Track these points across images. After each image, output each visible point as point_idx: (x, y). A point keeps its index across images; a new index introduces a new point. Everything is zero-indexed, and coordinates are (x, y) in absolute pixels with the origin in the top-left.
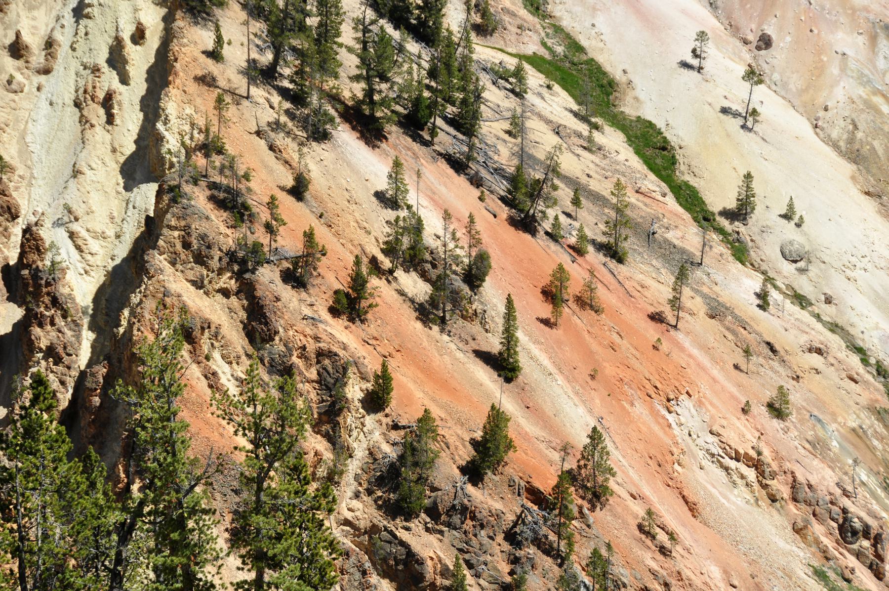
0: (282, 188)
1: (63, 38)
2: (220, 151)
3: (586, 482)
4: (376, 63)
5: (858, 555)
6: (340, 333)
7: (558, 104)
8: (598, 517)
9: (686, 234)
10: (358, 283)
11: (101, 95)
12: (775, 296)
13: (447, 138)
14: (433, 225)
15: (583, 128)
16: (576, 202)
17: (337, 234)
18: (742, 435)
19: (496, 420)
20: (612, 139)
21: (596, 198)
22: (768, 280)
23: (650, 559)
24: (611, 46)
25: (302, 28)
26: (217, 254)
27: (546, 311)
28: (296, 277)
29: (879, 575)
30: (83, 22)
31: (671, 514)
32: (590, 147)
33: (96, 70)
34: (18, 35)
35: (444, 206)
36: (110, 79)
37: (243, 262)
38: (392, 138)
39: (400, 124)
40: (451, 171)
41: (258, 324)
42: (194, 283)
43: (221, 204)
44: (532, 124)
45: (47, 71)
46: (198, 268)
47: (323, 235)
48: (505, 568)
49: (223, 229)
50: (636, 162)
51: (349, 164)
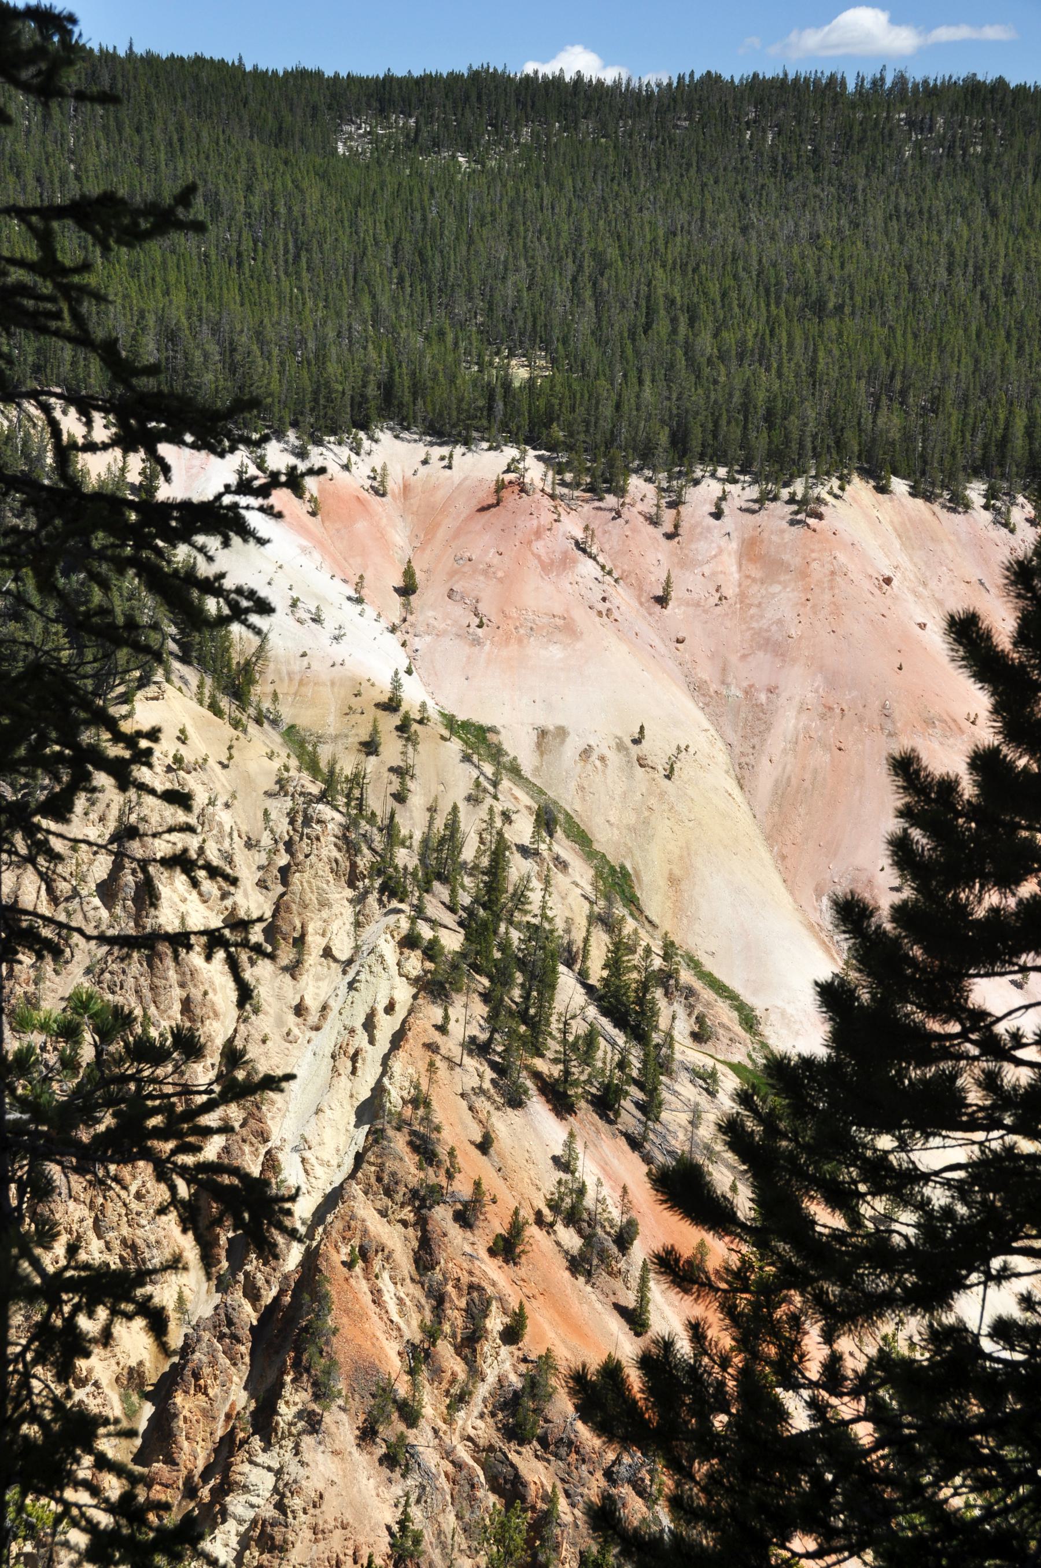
0: (472, 1143)
1: (335, 1005)
11: (351, 1051)
17: (511, 1187)
26: (402, 1190)
30: (353, 993)
33: (352, 1031)
34: (302, 998)
36: (361, 1039)
37: (423, 1200)
38: (580, 1114)
39: (591, 1103)
40: (626, 1148)
42: (380, 1212)
46: (385, 1199)
49: (413, 1170)
51: (535, 1129)
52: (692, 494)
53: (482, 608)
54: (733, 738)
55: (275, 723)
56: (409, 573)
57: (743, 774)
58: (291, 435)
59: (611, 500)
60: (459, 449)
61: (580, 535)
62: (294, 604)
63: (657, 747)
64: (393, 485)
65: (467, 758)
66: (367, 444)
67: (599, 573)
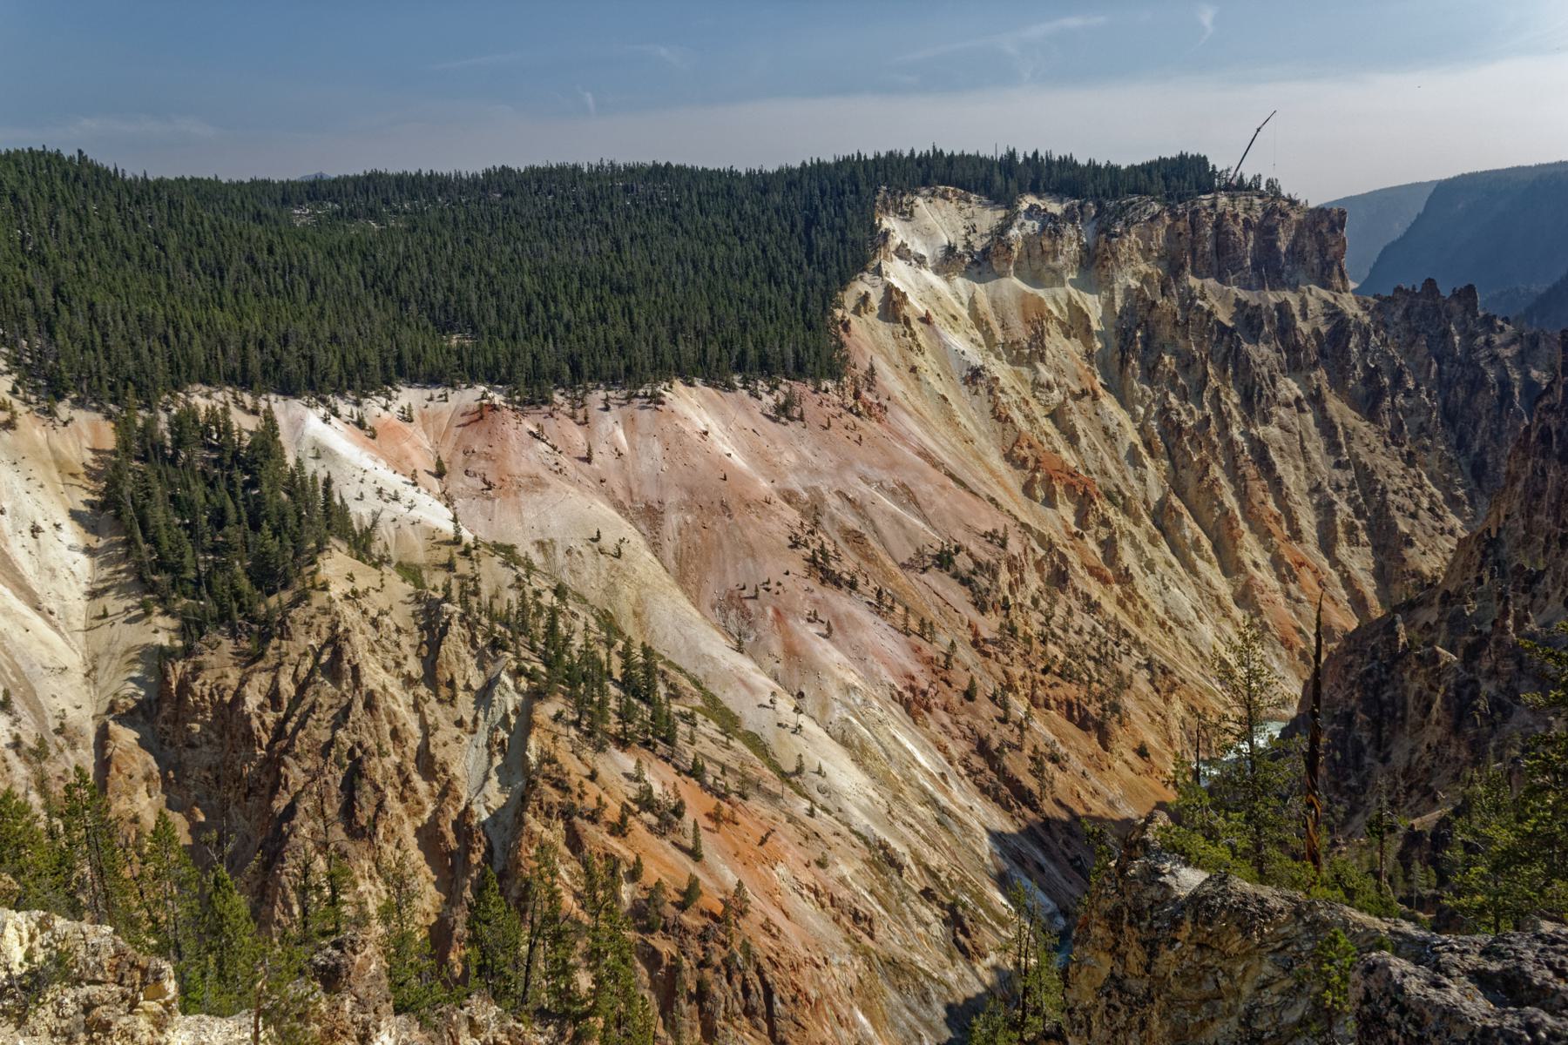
2: (555, 762)
3: (736, 905)
4: (625, 715)
5: (863, 930)
6: (614, 844)
7: (709, 728)
8: (742, 922)
9: (774, 785)
10: (623, 819)
12: (818, 810)
13: (662, 748)
14: (657, 789)
15: (724, 739)
16: (723, 772)
18: (806, 877)
19: (694, 883)
20: (736, 743)
21: (733, 771)
22: (813, 802)
23: (768, 941)
24: (732, 699)
25: (592, 702)
27: (711, 825)
28: (593, 818)
29: (872, 937)
31: (777, 917)
32: (728, 747)
35: (660, 778)
41: (575, 842)
43: (555, 786)
44: (699, 738)
45: (474, 732)
47: (605, 798)
48: (701, 954)
50: (749, 753)
52: (590, 398)
53: (488, 478)
54: (643, 527)
55: (389, 562)
56: (439, 464)
57: (655, 547)
58: (348, 393)
59: (546, 408)
60: (449, 391)
61: (535, 430)
62: (380, 491)
63: (608, 541)
64: (415, 414)
65: (506, 564)
66: (394, 394)
67: (550, 450)
